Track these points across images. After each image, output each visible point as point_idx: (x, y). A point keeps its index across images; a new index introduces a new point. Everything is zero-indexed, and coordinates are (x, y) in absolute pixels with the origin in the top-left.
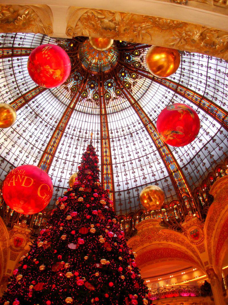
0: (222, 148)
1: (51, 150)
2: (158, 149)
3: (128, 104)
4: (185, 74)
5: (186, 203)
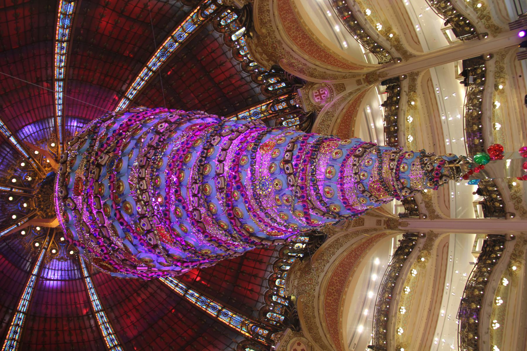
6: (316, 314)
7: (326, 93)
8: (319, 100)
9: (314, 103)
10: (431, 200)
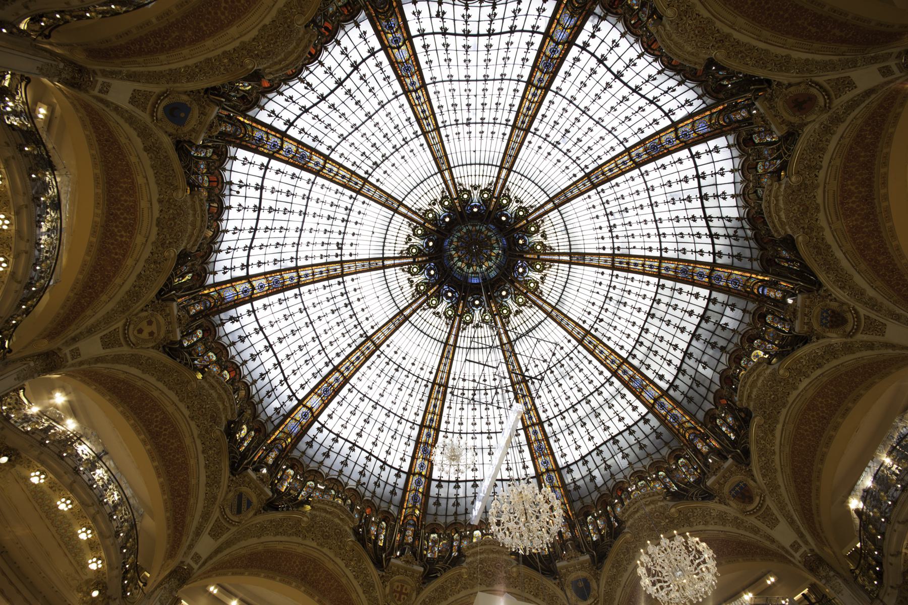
0: (726, 324)
1: (432, 420)
2: (614, 373)
3: (543, 316)
4: (620, 234)
5: (699, 446)
6: (160, 385)
8: (395, 587)
9: (396, 578)
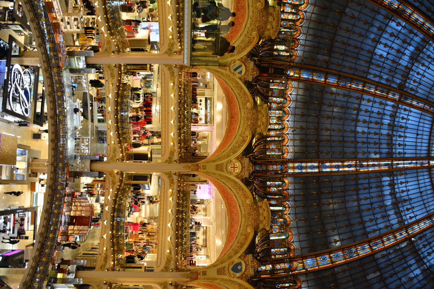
7: (230, 168)
8: (236, 164)
10: (171, 77)
